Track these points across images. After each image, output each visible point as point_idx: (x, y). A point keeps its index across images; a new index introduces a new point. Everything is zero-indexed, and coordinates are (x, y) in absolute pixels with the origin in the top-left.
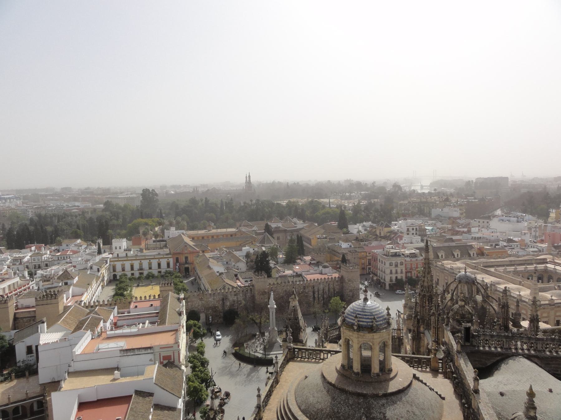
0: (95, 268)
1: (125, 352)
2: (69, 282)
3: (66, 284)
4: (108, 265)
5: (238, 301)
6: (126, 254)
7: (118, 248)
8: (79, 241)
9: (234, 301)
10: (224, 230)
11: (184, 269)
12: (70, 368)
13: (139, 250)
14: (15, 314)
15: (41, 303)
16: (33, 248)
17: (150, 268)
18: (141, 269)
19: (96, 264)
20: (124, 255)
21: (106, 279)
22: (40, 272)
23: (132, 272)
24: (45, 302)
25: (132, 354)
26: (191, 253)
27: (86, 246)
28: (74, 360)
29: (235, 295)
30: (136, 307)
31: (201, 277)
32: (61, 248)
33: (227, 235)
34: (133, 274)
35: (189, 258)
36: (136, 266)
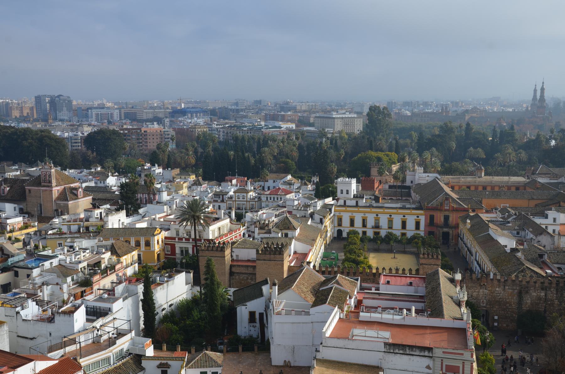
0: (317, 217)
1: (392, 347)
2: (290, 233)
3: (286, 235)
4: (332, 215)
5: (546, 300)
6: (357, 202)
7: (345, 192)
8: (289, 177)
9: (539, 298)
10: (506, 178)
11: (441, 234)
12: (318, 354)
13: (373, 197)
14: (231, 266)
15: (262, 257)
16: (234, 181)
17: (390, 227)
18: (377, 226)
19: (319, 212)
20: (353, 203)
21: (329, 235)
22: (249, 215)
23: (364, 229)
24: (268, 257)
25: (401, 352)
26: (454, 210)
27: (299, 185)
28: (324, 344)
29: (542, 289)
30: (388, 282)
31: (473, 251)
32: (267, 185)
33: (509, 188)
34: (364, 233)
35: (451, 219)
36: (371, 222)
